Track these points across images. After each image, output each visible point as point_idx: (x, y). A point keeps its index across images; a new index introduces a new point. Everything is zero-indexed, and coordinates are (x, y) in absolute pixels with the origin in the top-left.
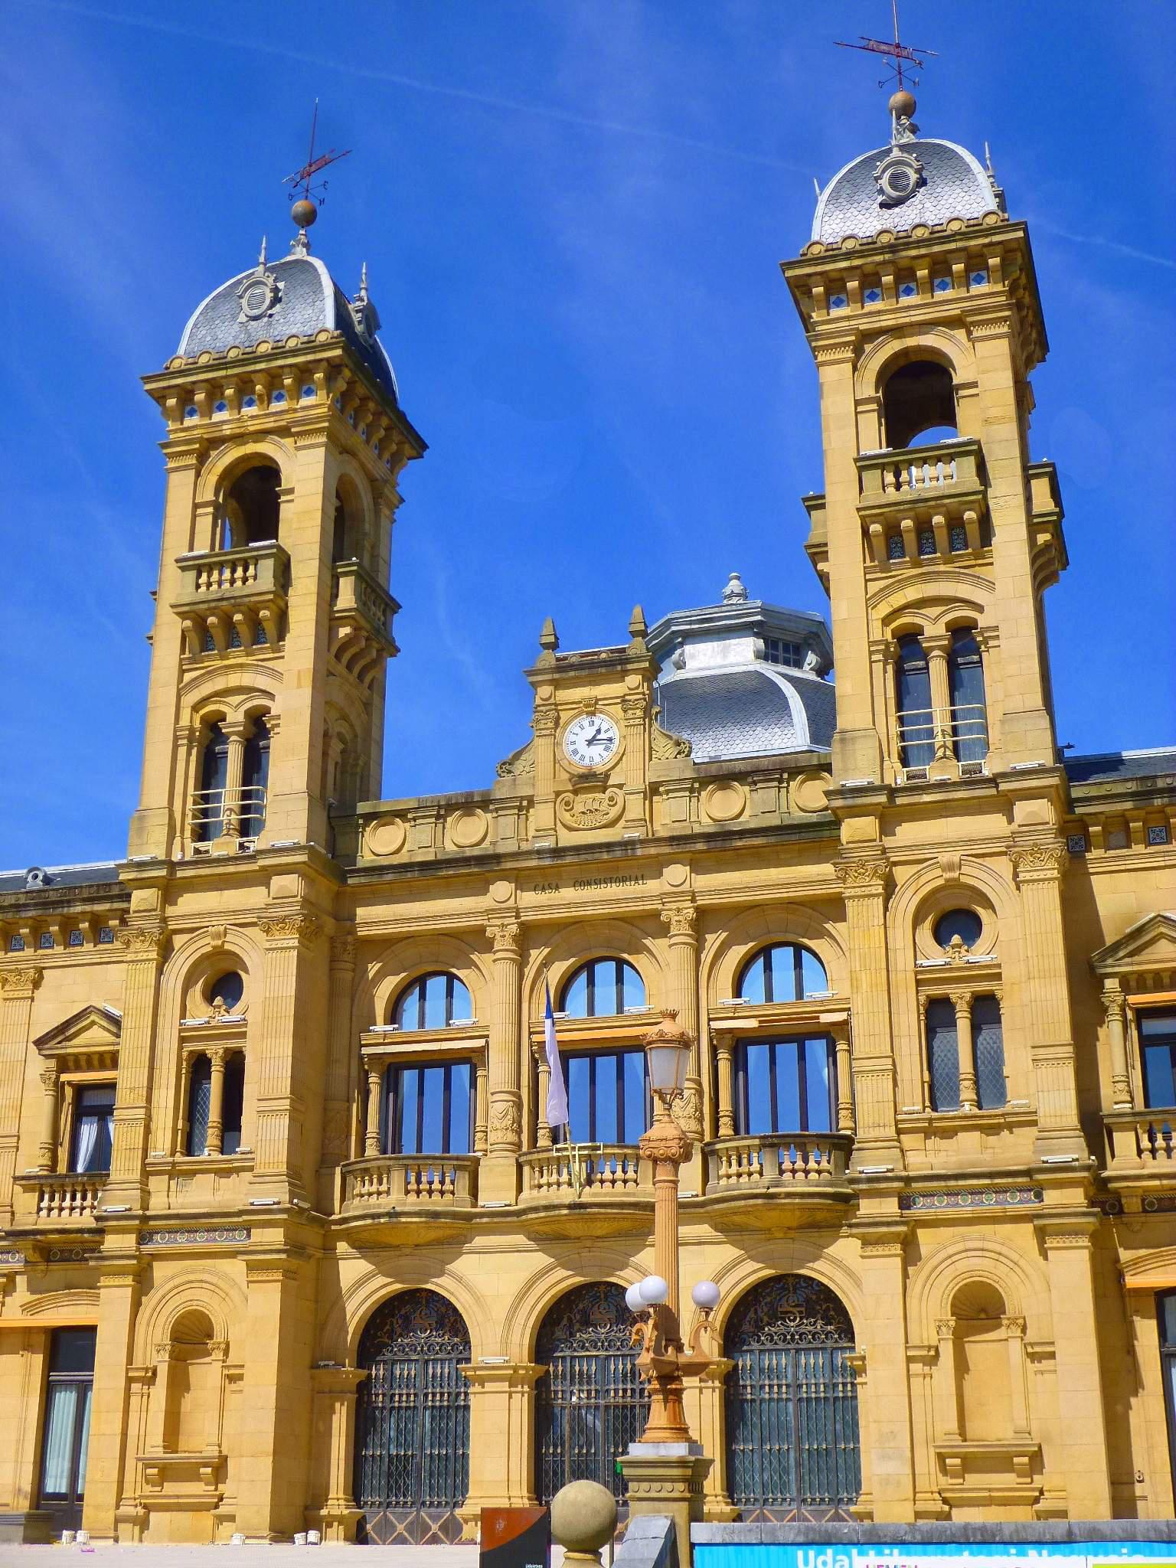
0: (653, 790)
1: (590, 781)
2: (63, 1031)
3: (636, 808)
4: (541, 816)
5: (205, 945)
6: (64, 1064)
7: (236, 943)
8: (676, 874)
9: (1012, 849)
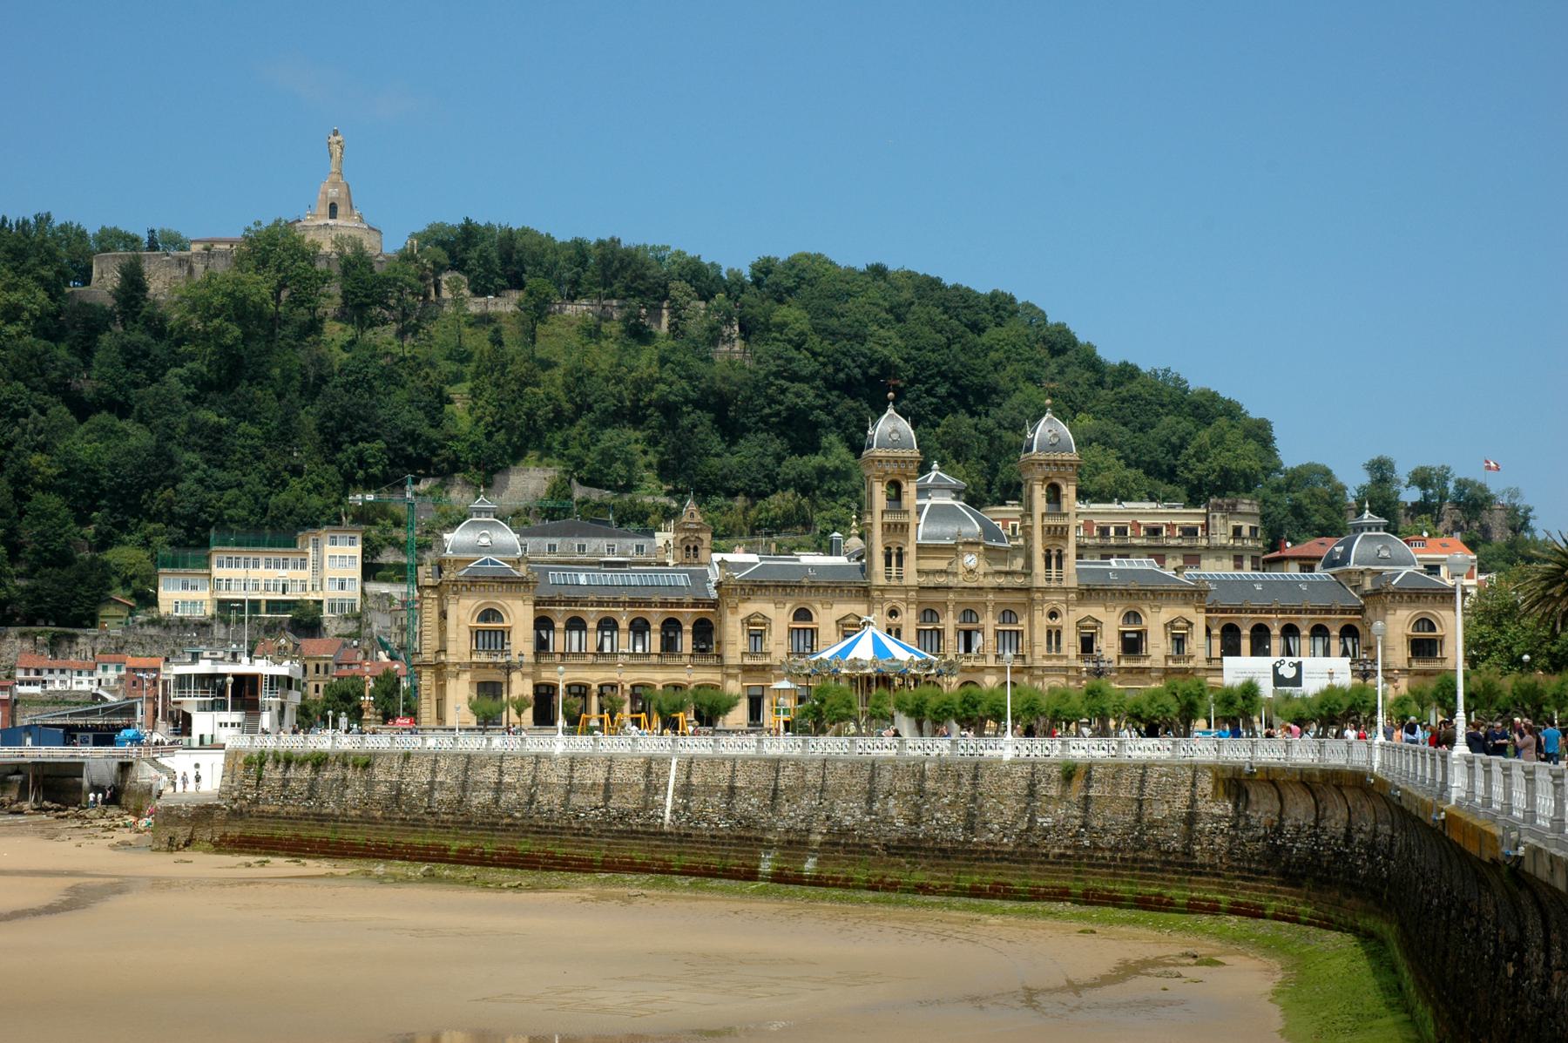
0: (985, 575)
1: (971, 571)
2: (844, 618)
3: (981, 578)
4: (960, 578)
5: (890, 605)
6: (844, 625)
7: (898, 605)
8: (991, 596)
9: (1067, 602)
